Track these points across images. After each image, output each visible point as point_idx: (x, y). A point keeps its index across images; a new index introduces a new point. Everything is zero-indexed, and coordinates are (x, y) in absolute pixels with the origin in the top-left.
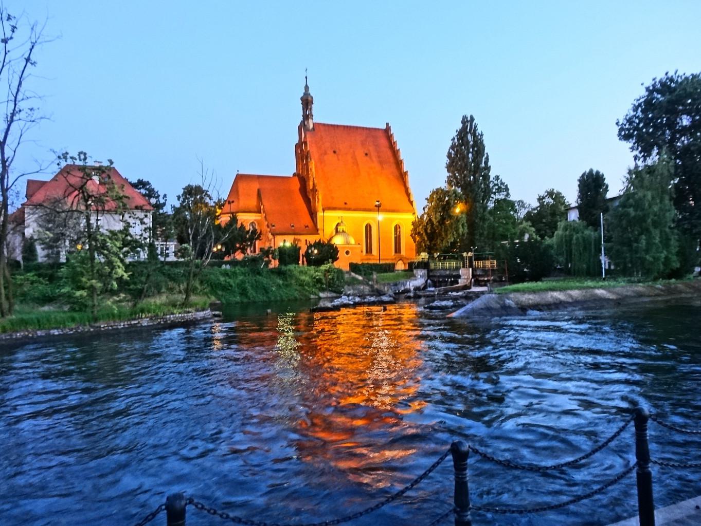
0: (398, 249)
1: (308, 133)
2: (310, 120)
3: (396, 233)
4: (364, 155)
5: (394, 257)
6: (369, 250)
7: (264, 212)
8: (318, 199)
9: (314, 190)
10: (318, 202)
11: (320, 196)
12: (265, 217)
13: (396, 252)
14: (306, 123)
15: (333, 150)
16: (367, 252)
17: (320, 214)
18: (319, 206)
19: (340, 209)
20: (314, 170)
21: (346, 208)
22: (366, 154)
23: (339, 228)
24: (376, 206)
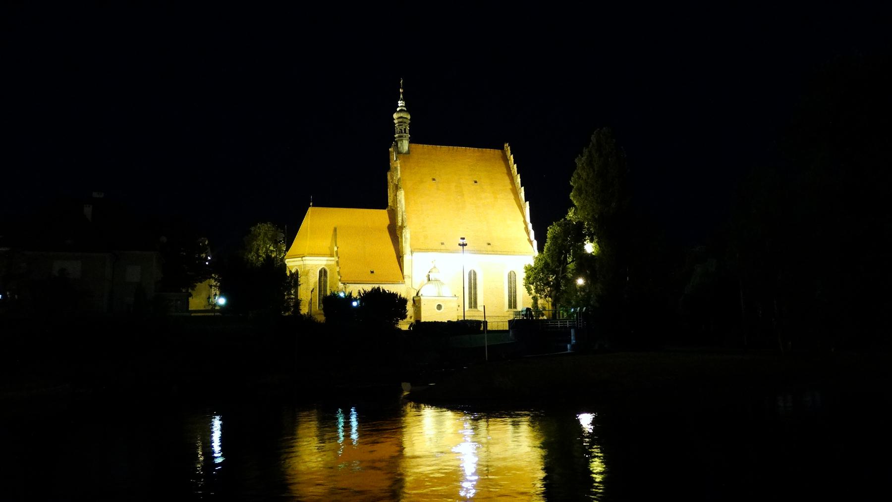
0: (512, 304)
2: (404, 141)
3: (510, 282)
4: (474, 182)
5: (507, 314)
6: (473, 304)
7: (337, 254)
8: (406, 238)
9: (402, 227)
10: (405, 242)
12: (337, 262)
13: (510, 307)
14: (399, 145)
16: (469, 308)
17: (407, 259)
18: (406, 247)
19: (436, 250)
20: (403, 201)
21: (442, 248)
22: (476, 182)
23: (430, 274)
24: (460, 245)
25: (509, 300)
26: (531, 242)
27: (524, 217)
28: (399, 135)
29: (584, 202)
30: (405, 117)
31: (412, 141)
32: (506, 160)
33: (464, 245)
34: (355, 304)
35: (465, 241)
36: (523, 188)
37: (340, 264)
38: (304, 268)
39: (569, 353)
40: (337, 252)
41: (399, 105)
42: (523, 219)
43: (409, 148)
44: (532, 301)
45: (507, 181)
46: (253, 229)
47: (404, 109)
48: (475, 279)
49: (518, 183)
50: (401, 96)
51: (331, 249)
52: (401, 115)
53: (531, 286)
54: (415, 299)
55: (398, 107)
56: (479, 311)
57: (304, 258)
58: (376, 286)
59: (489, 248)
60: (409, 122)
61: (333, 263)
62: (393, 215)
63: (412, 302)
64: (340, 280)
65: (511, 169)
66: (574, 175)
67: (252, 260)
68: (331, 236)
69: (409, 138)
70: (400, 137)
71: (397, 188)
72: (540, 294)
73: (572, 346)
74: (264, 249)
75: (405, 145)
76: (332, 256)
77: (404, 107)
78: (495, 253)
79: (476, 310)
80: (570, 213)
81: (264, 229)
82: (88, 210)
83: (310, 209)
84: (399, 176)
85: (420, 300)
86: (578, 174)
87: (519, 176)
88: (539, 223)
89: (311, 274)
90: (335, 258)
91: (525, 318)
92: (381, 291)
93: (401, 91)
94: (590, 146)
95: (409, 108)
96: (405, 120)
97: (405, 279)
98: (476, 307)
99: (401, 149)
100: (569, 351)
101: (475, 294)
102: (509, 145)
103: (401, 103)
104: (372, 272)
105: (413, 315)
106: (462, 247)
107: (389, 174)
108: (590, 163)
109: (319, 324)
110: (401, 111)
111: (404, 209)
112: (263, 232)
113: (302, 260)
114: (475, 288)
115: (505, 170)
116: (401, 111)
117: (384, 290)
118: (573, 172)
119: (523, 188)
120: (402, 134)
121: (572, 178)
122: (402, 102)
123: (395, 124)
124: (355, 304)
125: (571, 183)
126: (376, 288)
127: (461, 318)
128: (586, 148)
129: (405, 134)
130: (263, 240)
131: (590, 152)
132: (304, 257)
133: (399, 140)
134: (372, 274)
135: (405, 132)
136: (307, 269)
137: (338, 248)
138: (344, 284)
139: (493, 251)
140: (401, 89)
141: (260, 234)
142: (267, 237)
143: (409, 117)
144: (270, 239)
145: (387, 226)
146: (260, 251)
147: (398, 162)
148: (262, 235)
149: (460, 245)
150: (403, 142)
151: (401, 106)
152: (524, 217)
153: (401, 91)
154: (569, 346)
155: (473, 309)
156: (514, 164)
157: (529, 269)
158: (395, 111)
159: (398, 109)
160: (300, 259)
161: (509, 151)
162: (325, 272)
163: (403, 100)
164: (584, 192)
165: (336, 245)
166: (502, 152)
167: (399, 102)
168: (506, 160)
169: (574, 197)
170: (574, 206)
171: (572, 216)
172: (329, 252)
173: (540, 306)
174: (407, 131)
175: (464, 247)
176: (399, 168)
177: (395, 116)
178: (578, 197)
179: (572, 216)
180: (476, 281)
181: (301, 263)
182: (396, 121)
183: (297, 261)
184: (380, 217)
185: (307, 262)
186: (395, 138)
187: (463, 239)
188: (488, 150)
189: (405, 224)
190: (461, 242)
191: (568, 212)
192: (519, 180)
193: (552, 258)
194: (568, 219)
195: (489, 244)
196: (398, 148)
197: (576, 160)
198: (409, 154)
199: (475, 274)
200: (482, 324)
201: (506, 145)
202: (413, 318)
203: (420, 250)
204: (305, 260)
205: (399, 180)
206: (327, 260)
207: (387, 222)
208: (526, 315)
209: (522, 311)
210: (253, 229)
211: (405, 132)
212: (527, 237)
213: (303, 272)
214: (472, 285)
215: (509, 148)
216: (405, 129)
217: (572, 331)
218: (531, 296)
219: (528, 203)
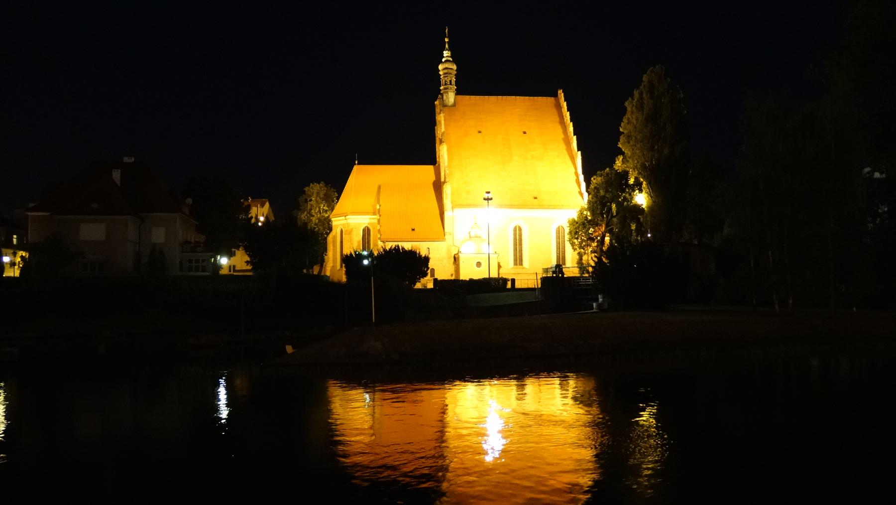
1: (446, 109)
2: (450, 93)
9: (445, 182)
11: (447, 190)
12: (379, 221)
14: (445, 97)
15: (478, 130)
16: (515, 264)
22: (525, 133)
24: (485, 199)
25: (557, 256)
26: (581, 194)
27: (576, 168)
28: (444, 86)
29: (633, 150)
30: (450, 67)
31: (459, 92)
32: (559, 107)
33: (488, 199)
34: (366, 262)
35: (490, 196)
37: (381, 221)
38: (348, 226)
39: (595, 312)
40: (379, 210)
41: (445, 55)
42: (574, 170)
44: (578, 257)
45: (559, 130)
46: (306, 189)
47: (451, 60)
48: (520, 235)
49: (570, 132)
50: (447, 46)
51: (374, 207)
52: (447, 67)
53: (575, 241)
54: (456, 256)
55: (444, 57)
56: (524, 268)
57: (347, 217)
58: (396, 243)
59: (535, 202)
60: (456, 72)
61: (376, 221)
62: (438, 173)
63: (453, 259)
64: (380, 239)
65: (564, 117)
66: (624, 120)
67: (304, 220)
68: (375, 194)
69: (456, 90)
70: (445, 89)
71: (441, 142)
72: (584, 249)
73: (599, 306)
74: (318, 209)
75: (450, 97)
76: (376, 215)
77: (450, 57)
78: (541, 207)
79: (521, 267)
80: (617, 162)
81: (316, 190)
82: (116, 175)
83: (355, 167)
84: (443, 129)
85: (458, 258)
86: (628, 119)
87: (571, 124)
88: (588, 173)
89: (354, 233)
90: (377, 217)
91: (554, 275)
92: (401, 248)
93: (447, 40)
94: (641, 87)
95: (455, 59)
96: (450, 71)
97: (446, 237)
98: (521, 264)
99: (446, 102)
100: (594, 311)
101: (521, 251)
102: (563, 92)
103: (446, 53)
104: (413, 230)
105: (454, 273)
106: (487, 201)
107: (436, 127)
108: (640, 107)
109: (339, 284)
110: (446, 61)
111: (446, 164)
112: (315, 191)
113: (346, 219)
114: (521, 244)
115: (557, 119)
117: (403, 248)
118: (623, 118)
120: (446, 86)
121: (622, 124)
122: (447, 52)
123: (440, 75)
124: (366, 262)
125: (621, 130)
126: (394, 247)
127: (488, 277)
128: (636, 90)
129: (450, 86)
130: (316, 200)
131: (641, 94)
132: (347, 215)
133: (444, 92)
134: (413, 231)
135: (451, 84)
136: (350, 228)
137: (380, 206)
138: (383, 242)
139: (533, 206)
140: (446, 39)
141: (313, 194)
142: (320, 197)
143: (455, 67)
144: (323, 199)
145: (432, 182)
146: (313, 211)
147: (442, 115)
148: (315, 195)
149: (485, 199)
150: (448, 94)
151: (446, 57)
152: (576, 168)
153: (446, 40)
154: (595, 305)
155: (518, 266)
157: (573, 223)
158: (441, 62)
160: (343, 218)
161: (563, 98)
162: (369, 230)
163: (450, 49)
164: (634, 138)
165: (379, 202)
166: (555, 99)
167: (445, 52)
168: (559, 107)
169: (623, 144)
170: (623, 153)
171: (620, 165)
172: (372, 211)
173: (584, 262)
174: (453, 82)
175: (489, 201)
176: (443, 122)
177: (441, 67)
178: (627, 144)
179: (620, 165)
180: (521, 237)
181: (345, 222)
182: (441, 73)
183: (339, 220)
184: (425, 172)
185: (349, 221)
186: (441, 90)
187: (488, 193)
188: (540, 98)
189: (447, 180)
190: (486, 196)
191: (615, 161)
192: (571, 129)
193: (593, 211)
194: (616, 168)
195: (535, 198)
196: (443, 101)
197: (626, 104)
198: (455, 106)
199: (520, 229)
200: (509, 284)
201: (560, 92)
202: (454, 276)
203: (462, 206)
204: (348, 219)
205: (443, 134)
206: (370, 219)
207: (433, 178)
208: (554, 272)
209: (551, 268)
210: (306, 189)
211: (451, 84)
212: (579, 190)
213: (347, 231)
214: (518, 241)
215: (563, 94)
216: (450, 81)
218: (577, 252)
219: (580, 152)
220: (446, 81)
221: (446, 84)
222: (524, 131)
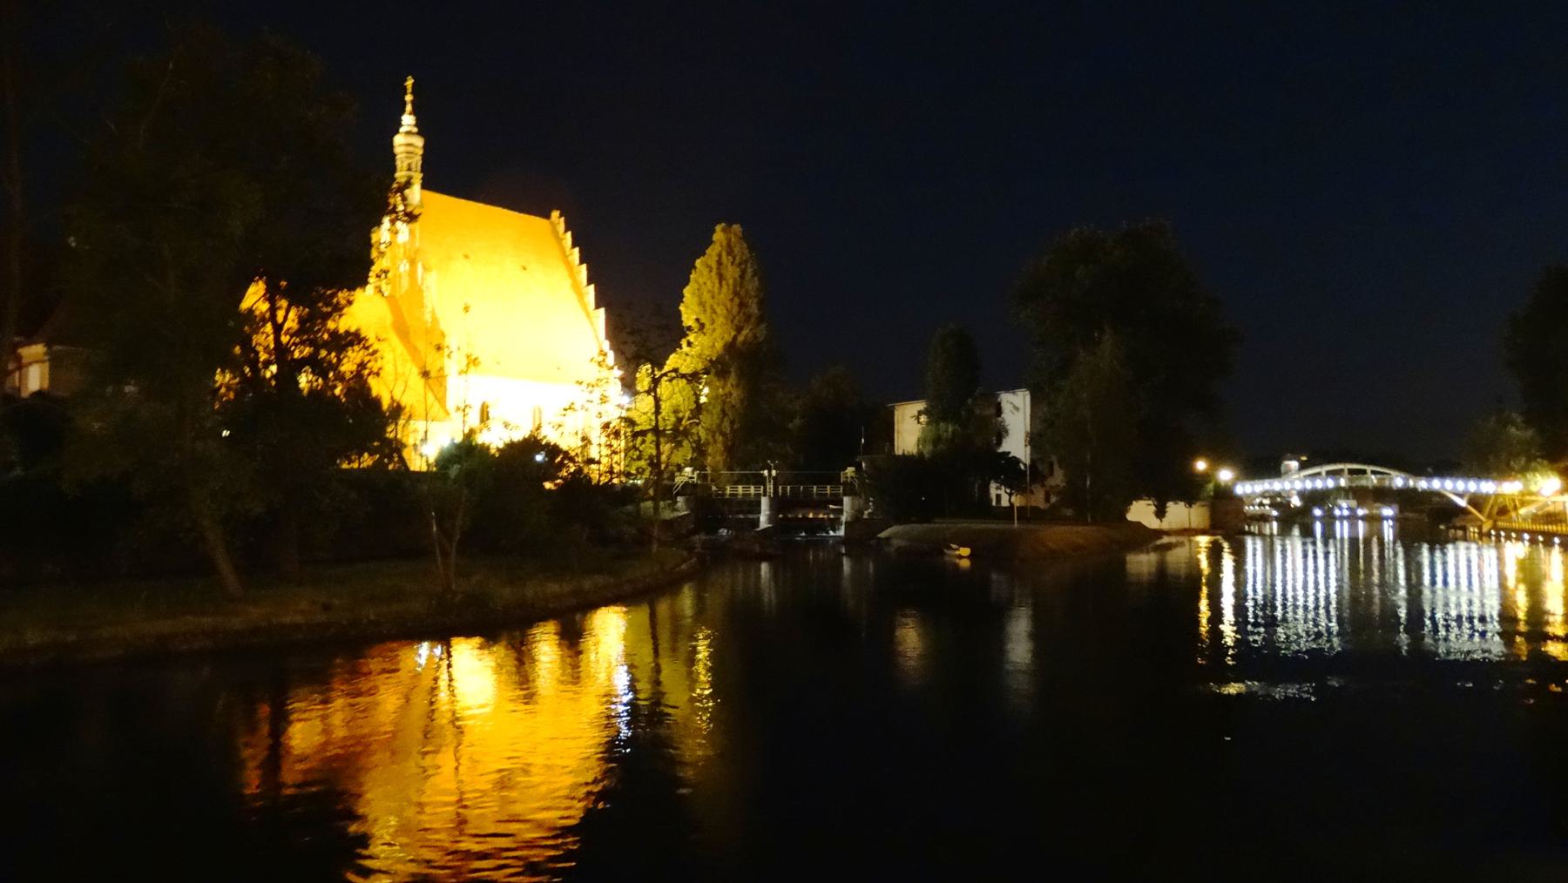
27: (595, 330)
31: (426, 185)
32: (559, 240)
36: (592, 286)
43: (421, 198)
45: (566, 274)
52: (407, 143)
65: (568, 253)
75: (416, 193)
84: (417, 245)
95: (423, 128)
103: (408, 120)
110: (409, 133)
116: (409, 133)
119: (592, 286)
156: (574, 246)
159: (402, 130)
163: (414, 112)
168: (559, 240)
177: (398, 140)
217: (765, 502)
220: (409, 165)
221: (409, 169)
222: (524, 265)
